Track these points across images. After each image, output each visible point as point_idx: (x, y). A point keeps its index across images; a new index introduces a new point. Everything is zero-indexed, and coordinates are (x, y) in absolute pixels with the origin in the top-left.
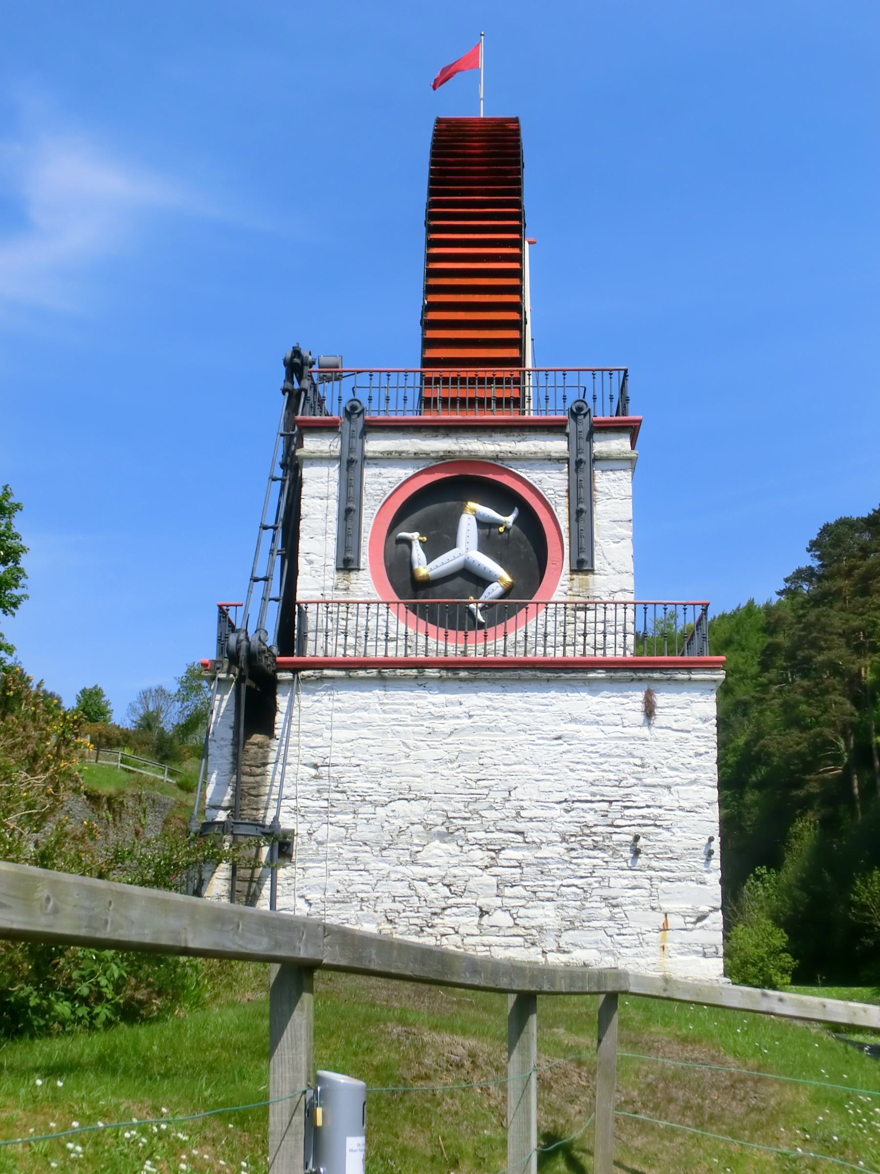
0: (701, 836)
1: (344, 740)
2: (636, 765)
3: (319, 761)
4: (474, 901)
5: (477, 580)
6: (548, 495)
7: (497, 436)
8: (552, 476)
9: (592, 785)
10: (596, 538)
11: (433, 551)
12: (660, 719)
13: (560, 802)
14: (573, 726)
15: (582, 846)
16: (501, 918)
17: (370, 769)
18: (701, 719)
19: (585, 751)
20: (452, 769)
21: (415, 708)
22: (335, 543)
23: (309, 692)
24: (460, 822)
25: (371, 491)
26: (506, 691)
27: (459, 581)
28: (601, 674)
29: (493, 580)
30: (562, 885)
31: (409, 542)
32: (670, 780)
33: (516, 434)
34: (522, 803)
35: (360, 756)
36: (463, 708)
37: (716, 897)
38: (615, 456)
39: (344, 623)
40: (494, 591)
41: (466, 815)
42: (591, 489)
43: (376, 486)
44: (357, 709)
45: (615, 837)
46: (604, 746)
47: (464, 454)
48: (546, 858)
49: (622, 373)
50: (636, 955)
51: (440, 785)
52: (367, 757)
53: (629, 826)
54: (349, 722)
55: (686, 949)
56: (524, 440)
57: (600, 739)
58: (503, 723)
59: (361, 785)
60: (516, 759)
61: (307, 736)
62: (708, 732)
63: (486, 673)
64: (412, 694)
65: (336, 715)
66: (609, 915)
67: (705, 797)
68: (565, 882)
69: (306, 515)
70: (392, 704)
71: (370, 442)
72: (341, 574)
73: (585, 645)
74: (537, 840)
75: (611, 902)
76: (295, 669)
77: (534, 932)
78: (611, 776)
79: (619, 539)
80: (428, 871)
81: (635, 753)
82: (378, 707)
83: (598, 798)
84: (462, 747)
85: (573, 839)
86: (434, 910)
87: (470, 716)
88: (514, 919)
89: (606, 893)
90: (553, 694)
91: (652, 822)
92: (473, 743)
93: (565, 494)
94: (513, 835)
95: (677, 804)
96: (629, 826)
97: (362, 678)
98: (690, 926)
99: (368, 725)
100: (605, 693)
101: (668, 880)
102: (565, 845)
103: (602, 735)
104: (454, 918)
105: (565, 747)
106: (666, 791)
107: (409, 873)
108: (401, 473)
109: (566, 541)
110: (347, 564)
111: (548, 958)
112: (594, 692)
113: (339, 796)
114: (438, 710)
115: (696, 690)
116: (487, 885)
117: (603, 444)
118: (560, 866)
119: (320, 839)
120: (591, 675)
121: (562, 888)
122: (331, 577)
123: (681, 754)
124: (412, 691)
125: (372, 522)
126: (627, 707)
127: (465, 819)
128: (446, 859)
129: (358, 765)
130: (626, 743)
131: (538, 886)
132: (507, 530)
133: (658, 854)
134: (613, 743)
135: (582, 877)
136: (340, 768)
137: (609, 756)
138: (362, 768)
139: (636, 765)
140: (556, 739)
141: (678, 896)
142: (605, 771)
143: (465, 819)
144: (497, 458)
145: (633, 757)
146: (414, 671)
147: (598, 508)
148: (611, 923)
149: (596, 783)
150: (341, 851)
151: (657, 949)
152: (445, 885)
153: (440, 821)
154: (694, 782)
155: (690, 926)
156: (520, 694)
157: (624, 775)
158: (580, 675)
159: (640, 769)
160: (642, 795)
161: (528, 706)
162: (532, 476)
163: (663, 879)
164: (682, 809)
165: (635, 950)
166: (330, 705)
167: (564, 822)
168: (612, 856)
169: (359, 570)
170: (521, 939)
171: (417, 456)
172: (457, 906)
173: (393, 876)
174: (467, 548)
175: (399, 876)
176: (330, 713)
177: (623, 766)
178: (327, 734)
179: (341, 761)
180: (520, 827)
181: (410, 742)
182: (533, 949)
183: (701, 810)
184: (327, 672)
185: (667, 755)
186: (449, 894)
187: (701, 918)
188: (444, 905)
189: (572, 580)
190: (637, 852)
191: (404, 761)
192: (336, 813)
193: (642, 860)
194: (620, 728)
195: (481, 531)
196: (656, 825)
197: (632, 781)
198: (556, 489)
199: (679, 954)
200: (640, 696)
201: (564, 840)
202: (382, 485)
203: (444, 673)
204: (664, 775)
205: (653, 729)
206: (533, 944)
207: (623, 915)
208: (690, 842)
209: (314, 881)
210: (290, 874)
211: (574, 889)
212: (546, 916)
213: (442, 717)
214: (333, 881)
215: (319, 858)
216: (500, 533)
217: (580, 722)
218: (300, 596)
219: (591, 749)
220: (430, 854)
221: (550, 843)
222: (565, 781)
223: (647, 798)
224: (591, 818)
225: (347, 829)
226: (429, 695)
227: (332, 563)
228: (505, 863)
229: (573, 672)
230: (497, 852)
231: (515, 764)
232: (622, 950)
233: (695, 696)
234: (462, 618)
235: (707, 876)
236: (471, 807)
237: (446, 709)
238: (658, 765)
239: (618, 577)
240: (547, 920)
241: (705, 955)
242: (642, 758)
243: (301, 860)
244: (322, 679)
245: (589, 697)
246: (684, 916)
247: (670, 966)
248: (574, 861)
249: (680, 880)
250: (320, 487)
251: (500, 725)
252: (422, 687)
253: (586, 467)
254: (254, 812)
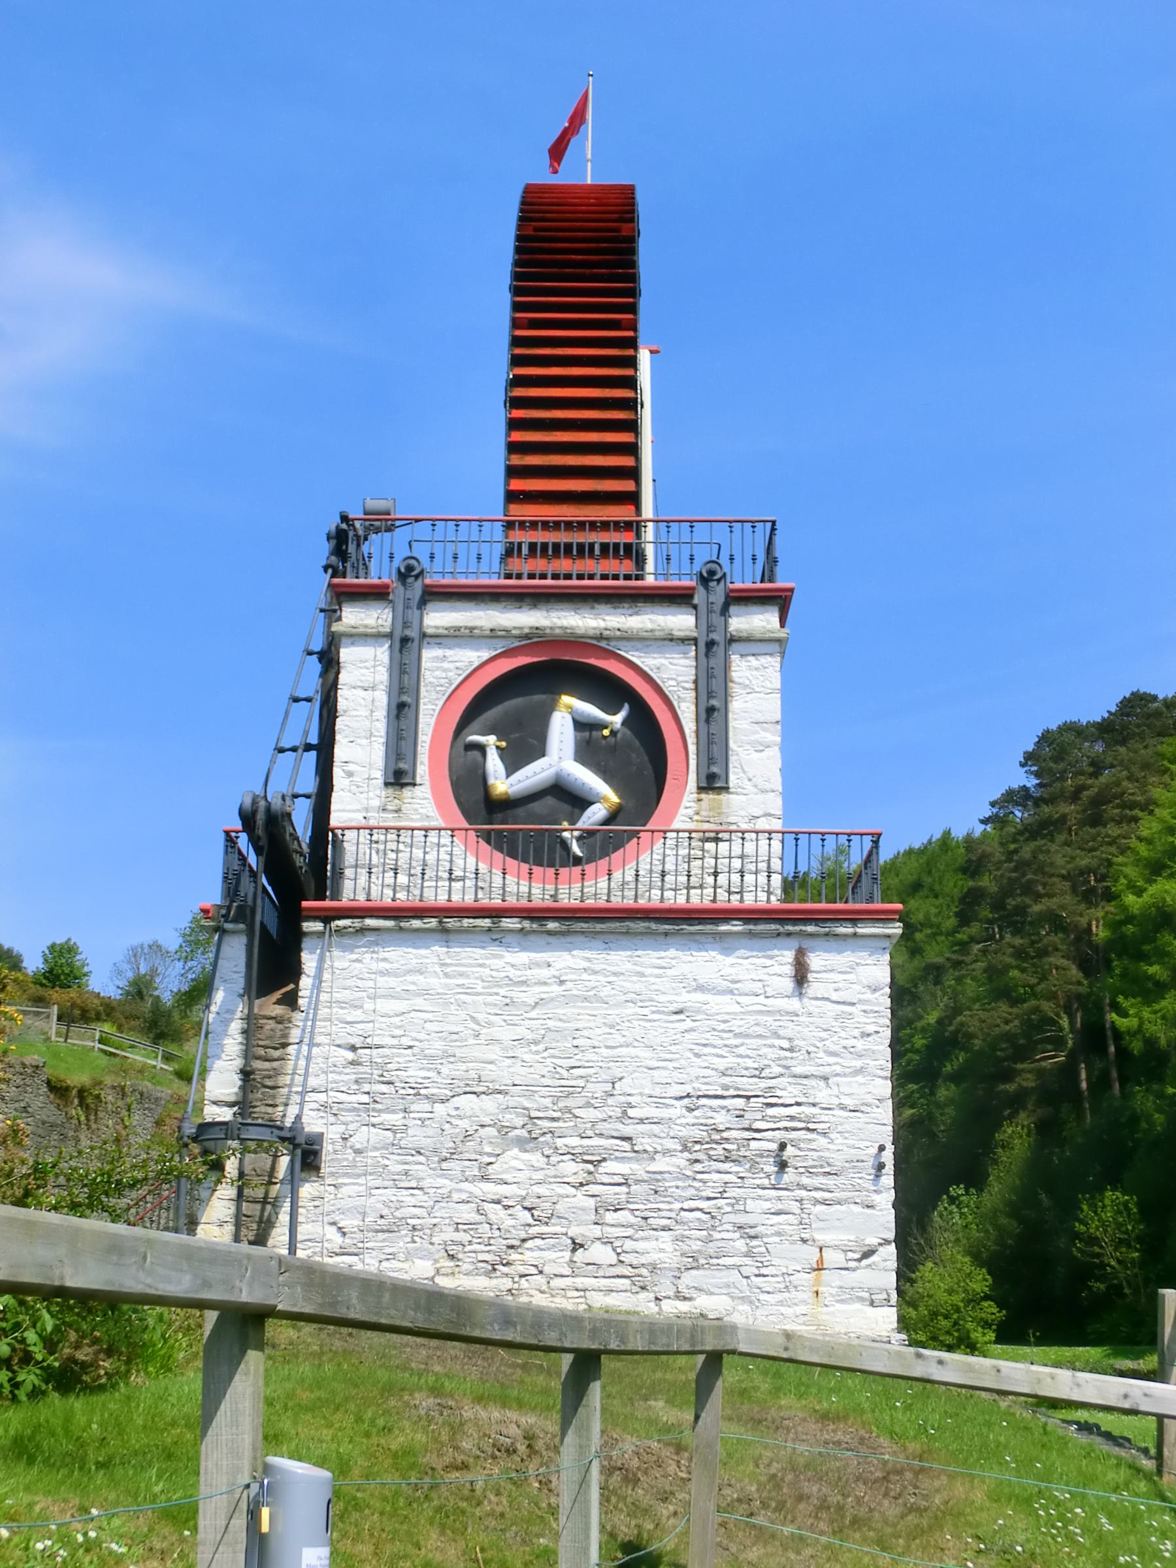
0: (868, 1144)
1: (392, 1013)
2: (782, 1049)
3: (357, 1041)
4: (564, 1230)
5: (574, 800)
6: (669, 687)
7: (602, 608)
8: (675, 661)
9: (724, 1075)
10: (732, 744)
11: (514, 760)
12: (814, 987)
13: (682, 1098)
14: (699, 997)
15: (710, 1157)
16: (601, 1253)
17: (427, 1052)
18: (869, 987)
19: (714, 1030)
20: (537, 1053)
21: (487, 971)
22: (383, 748)
23: (344, 948)
24: (546, 1124)
25: (432, 680)
26: (610, 949)
27: (550, 801)
28: (736, 927)
29: (593, 799)
30: (682, 1209)
31: (481, 748)
32: (827, 1069)
33: (626, 605)
34: (630, 1099)
35: (414, 1035)
36: (552, 971)
37: (887, 1225)
38: (758, 636)
39: (393, 856)
40: (595, 814)
41: (555, 1115)
42: (726, 679)
43: (438, 673)
44: (409, 972)
45: (753, 1144)
46: (741, 1023)
47: (557, 631)
48: (661, 1173)
49: (769, 525)
50: (781, 1303)
51: (520, 1073)
52: (422, 1036)
53: (773, 1130)
54: (398, 989)
55: (847, 1295)
56: (637, 614)
57: (735, 1014)
58: (605, 992)
59: (415, 1074)
60: (622, 1040)
61: (342, 1008)
62: (879, 1004)
63: (583, 925)
64: (483, 952)
65: (381, 981)
66: (745, 1249)
67: (875, 1092)
68: (686, 1205)
69: (345, 711)
70: (456, 965)
71: (432, 615)
72: (390, 791)
73: (715, 887)
74: (650, 1149)
75: (747, 1232)
76: (327, 917)
77: (644, 1271)
78: (750, 1063)
79: (763, 747)
80: (503, 1190)
81: (781, 1032)
82: (438, 969)
83: (732, 1092)
84: (551, 1023)
85: (697, 1147)
86: (510, 1242)
87: (562, 982)
88: (618, 1254)
89: (741, 1219)
90: (672, 952)
91: (803, 1125)
92: (564, 1018)
93: (692, 686)
94: (618, 1142)
95: (836, 1101)
96: (773, 1130)
97: (417, 930)
98: (853, 1264)
99: (425, 993)
100: (742, 952)
101: (824, 1202)
102: (686, 1154)
103: (737, 1009)
104: (537, 1254)
105: (689, 1024)
106: (822, 1083)
107: (478, 1192)
108: (473, 656)
109: (692, 748)
110: (399, 778)
111: (664, 1308)
112: (727, 951)
113: (384, 1088)
114: (518, 973)
115: (862, 948)
116: (583, 1209)
117: (742, 619)
118: (680, 1183)
119: (358, 1146)
120: (724, 928)
121: (683, 1213)
122: (377, 794)
123: (843, 1034)
124: (483, 948)
125: (433, 721)
126: (771, 970)
127: (553, 1119)
128: (527, 1174)
129: (410, 1047)
130: (770, 1019)
131: (651, 1210)
132: (613, 733)
133: (812, 1167)
134: (751, 1019)
135: (709, 1199)
136: (386, 1051)
137: (748, 1036)
138: (416, 1050)
139: (782, 1049)
140: (676, 1013)
141: (838, 1224)
142: (740, 1056)
143: (553, 1119)
144: (601, 637)
145: (779, 1037)
146: (487, 920)
147: (735, 705)
148: (747, 1261)
149: (729, 1072)
150: (386, 1162)
151: (808, 1296)
152: (525, 1208)
153: (519, 1122)
154: (860, 1071)
155: (853, 1264)
156: (629, 953)
157: (766, 1062)
158: (709, 928)
159: (788, 1054)
160: (790, 1089)
161: (639, 969)
162: (647, 661)
163: (817, 1202)
164: (843, 1107)
165: (779, 1297)
166: (374, 966)
167: (686, 1124)
168: (749, 1170)
169: (414, 785)
170: (626, 1282)
171: (493, 634)
172: (541, 1236)
173: (456, 1196)
174: (560, 757)
175: (464, 1196)
176: (373, 976)
177: (764, 1050)
178: (369, 1005)
179: (388, 1041)
180: (628, 1130)
181: (480, 1017)
182: (643, 1295)
183: (869, 1109)
184: (370, 922)
185: (824, 1035)
186: (531, 1221)
187: (868, 1254)
188: (523, 1235)
189: (700, 800)
190: (782, 1165)
191: (472, 1041)
192: (380, 1111)
193: (789, 1176)
194: (761, 999)
195: (579, 734)
196: (808, 1129)
197: (777, 1070)
198: (680, 679)
199: (837, 1301)
200: (789, 956)
201: (685, 1148)
202: (448, 671)
203: (527, 924)
204: (820, 1061)
205: (805, 1000)
206: (643, 1288)
207: (763, 1249)
208: (853, 1151)
209: (350, 1203)
210: (317, 1194)
211: (698, 1214)
212: (662, 1250)
213: (524, 983)
214: (375, 1203)
215: (357, 1171)
216: (605, 737)
217: (709, 991)
218: (335, 820)
219: (723, 1026)
220: (505, 1166)
221: (667, 1152)
222: (688, 1070)
223: (796, 1093)
224: (721, 1119)
225: (395, 1132)
226: (506, 954)
227: (379, 775)
228: (606, 1179)
229: (699, 924)
230: (597, 1163)
231: (621, 1046)
232: (763, 1297)
233: (862, 956)
234: (552, 851)
235: (877, 1198)
236: (561, 1104)
237: (529, 972)
238: (811, 1049)
239: (761, 797)
240: (661, 1255)
241: (872, 1303)
242: (790, 1039)
243: (332, 1174)
244: (362, 931)
245: (720, 957)
246: (845, 1251)
247: (825, 1317)
248: (699, 1176)
249: (839, 1203)
250: (364, 672)
251: (602, 994)
252: (497, 943)
253: (719, 650)
254: (270, 1110)
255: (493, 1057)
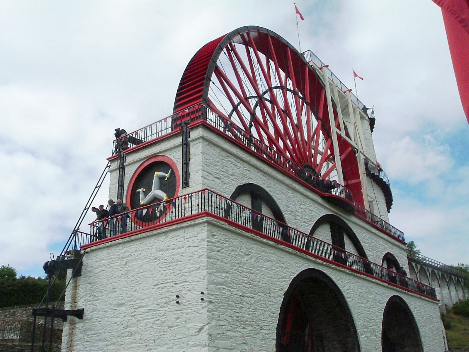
52: (103, 277)
103: (169, 255)
144: (160, 153)
155: (197, 333)
255: (116, 281)
